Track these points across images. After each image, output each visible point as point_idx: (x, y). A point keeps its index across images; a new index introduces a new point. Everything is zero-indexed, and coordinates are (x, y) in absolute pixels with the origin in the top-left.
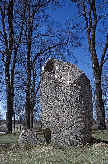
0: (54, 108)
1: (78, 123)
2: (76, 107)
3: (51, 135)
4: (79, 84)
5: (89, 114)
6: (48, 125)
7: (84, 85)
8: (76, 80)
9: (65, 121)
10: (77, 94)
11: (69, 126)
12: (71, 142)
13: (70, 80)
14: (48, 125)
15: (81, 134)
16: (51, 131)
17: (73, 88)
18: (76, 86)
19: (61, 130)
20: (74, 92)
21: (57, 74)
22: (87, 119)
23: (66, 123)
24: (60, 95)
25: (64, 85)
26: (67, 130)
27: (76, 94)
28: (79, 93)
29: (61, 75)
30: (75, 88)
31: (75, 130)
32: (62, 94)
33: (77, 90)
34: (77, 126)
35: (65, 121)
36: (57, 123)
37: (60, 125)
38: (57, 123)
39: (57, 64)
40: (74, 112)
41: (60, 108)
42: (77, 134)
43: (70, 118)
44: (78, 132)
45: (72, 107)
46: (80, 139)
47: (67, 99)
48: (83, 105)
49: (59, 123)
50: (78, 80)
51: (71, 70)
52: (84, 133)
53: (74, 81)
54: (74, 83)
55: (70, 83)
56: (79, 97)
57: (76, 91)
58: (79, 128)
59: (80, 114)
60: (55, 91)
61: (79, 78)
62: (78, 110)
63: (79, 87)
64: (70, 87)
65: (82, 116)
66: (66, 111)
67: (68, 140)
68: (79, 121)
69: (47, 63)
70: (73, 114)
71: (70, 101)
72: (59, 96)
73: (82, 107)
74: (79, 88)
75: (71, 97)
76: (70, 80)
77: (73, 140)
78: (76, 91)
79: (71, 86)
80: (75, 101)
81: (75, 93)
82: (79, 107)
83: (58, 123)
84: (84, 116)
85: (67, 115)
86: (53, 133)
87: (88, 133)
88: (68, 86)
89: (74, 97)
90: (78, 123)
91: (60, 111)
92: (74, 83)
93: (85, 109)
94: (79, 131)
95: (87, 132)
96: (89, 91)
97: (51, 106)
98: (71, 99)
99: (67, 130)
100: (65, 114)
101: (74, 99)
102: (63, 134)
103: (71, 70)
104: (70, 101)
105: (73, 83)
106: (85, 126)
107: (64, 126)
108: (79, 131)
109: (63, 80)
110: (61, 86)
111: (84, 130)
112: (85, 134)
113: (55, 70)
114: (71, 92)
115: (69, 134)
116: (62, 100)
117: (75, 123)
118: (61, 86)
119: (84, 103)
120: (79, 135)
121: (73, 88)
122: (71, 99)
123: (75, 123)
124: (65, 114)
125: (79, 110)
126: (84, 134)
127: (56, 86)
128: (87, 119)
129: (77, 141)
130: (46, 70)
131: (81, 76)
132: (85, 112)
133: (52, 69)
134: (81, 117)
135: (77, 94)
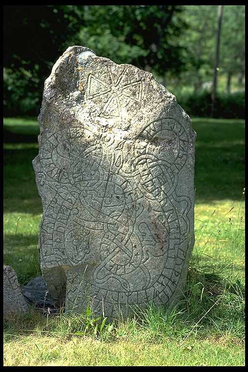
1: (145, 257)
3: (68, 286)
4: (153, 141)
5: (179, 227)
6: (58, 260)
7: (170, 142)
8: (144, 129)
9: (108, 250)
10: (146, 173)
13: (127, 129)
17: (134, 154)
18: (145, 147)
20: (137, 164)
21: (88, 103)
25: (110, 143)
27: (145, 170)
28: (152, 167)
29: (102, 108)
30: (141, 154)
33: (146, 159)
35: (108, 250)
43: (122, 241)
50: (150, 129)
51: (134, 94)
54: (140, 137)
55: (126, 139)
56: (151, 180)
57: (143, 164)
61: (157, 121)
64: (125, 151)
69: (61, 71)
74: (154, 153)
76: (127, 129)
78: (143, 164)
79: (129, 148)
87: (173, 283)
88: (119, 146)
89: (137, 181)
90: (145, 257)
92: (140, 137)
95: (170, 279)
96: (185, 157)
97: (67, 204)
99: (112, 275)
102: (100, 286)
105: (136, 139)
109: (106, 126)
111: (162, 275)
113: (84, 90)
117: (137, 255)
121: (137, 155)
123: (137, 255)
128: (172, 243)
130: (56, 95)
131: (160, 115)
132: (166, 225)
135: (146, 173)
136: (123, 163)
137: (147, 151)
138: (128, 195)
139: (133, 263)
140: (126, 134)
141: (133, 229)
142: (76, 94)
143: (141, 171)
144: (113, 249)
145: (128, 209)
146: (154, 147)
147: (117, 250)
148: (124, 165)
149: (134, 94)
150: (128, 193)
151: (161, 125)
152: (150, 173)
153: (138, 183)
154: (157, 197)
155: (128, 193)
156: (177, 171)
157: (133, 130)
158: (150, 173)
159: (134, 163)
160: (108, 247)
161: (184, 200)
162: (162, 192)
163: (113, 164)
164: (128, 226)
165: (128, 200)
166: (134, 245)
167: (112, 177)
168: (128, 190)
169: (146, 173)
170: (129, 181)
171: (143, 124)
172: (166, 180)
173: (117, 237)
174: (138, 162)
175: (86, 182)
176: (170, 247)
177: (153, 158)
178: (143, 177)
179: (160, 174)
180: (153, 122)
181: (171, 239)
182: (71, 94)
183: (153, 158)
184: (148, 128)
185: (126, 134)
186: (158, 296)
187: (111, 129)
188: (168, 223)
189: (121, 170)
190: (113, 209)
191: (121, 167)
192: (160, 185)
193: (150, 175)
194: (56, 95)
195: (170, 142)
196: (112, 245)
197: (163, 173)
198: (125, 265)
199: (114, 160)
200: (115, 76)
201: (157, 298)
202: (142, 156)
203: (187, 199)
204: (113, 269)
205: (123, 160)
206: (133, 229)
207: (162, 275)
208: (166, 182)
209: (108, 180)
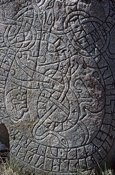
0: (13, 73)
1: (82, 114)
2: (75, 67)
3: (11, 142)
9: (45, 108)
10: (78, 29)
11: (56, 120)
12: (60, 162)
15: (91, 142)
16: (9, 132)
19: (34, 131)
20: (69, 21)
22: (108, 99)
23: (48, 113)
24: (29, 35)
25: (40, 3)
27: (77, 27)
28: (84, 23)
30: (72, 11)
31: (72, 132)
32: (34, 32)
33: (78, 15)
34: (79, 121)
36: (24, 112)
37: (32, 118)
38: (24, 112)
40: (69, 82)
41: (30, 72)
42: (79, 143)
43: (58, 99)
44: (81, 139)
45: (63, 67)
46: (87, 156)
47: (50, 44)
49: (29, 112)
52: (100, 140)
56: (84, 36)
57: (74, 20)
58: (83, 127)
59: (89, 86)
60: (15, 24)
62: (82, 76)
63: (85, 7)
64: (56, 9)
65: (93, 91)
66: (46, 79)
67: (53, 159)
68: (85, 107)
71: (57, 51)
72: (26, 38)
74: (86, 9)
75: (60, 38)
77: (66, 159)
78: (74, 20)
80: (72, 50)
81: (73, 25)
82: (84, 67)
83: (25, 114)
84: (100, 92)
85: (50, 90)
86: (14, 138)
87: (111, 137)
89: (70, 38)
90: (82, 114)
93: (102, 70)
94: (83, 136)
95: (108, 135)
98: (59, 45)
99: (51, 132)
100: (44, 88)
101: (68, 43)
102: (40, 141)
104: (57, 51)
106: (103, 120)
107: (41, 120)
108: (83, 136)
110: (32, 9)
111: (100, 130)
112: (102, 142)
114: (59, 22)
115: (55, 142)
116: (35, 47)
117: (74, 112)
118: (32, 9)
119: (101, 54)
120: (84, 145)
121: (67, 11)
122: (59, 45)
123: (74, 112)
124: (44, 88)
125: (85, 74)
126: (99, 141)
127: (17, 9)
129: (78, 162)
132: (102, 81)
134: (90, 95)
135: (78, 29)
136: (54, 21)
137: (78, 8)
138: (62, 53)
139: (70, 120)
141: (69, 87)
143: (73, 28)
144: (50, 107)
145: (63, 67)
146: (84, 4)
147: (54, 108)
148: (56, 22)
150: (61, 51)
152: (83, 30)
153: (71, 40)
154: (91, 54)
155: (61, 51)
156: (109, 29)
158: (83, 30)
159: (66, 20)
160: (45, 105)
163: (45, 23)
165: (61, 57)
166: (70, 102)
167: (44, 36)
168: (62, 48)
169: (79, 30)
170: (62, 38)
172: (99, 38)
173: (52, 95)
174: (70, 19)
176: (107, 103)
178: (76, 34)
179: (93, 31)
181: (107, 95)
183: (85, 14)
186: (97, 151)
188: (104, 80)
189: (53, 28)
191: (53, 25)
192: (93, 42)
193: (83, 31)
196: (48, 103)
197: (95, 29)
198: (62, 122)
199: (46, 18)
204: (51, 127)
205: (54, 18)
206: (69, 87)
207: (100, 130)
208: (99, 39)
209: (40, 39)
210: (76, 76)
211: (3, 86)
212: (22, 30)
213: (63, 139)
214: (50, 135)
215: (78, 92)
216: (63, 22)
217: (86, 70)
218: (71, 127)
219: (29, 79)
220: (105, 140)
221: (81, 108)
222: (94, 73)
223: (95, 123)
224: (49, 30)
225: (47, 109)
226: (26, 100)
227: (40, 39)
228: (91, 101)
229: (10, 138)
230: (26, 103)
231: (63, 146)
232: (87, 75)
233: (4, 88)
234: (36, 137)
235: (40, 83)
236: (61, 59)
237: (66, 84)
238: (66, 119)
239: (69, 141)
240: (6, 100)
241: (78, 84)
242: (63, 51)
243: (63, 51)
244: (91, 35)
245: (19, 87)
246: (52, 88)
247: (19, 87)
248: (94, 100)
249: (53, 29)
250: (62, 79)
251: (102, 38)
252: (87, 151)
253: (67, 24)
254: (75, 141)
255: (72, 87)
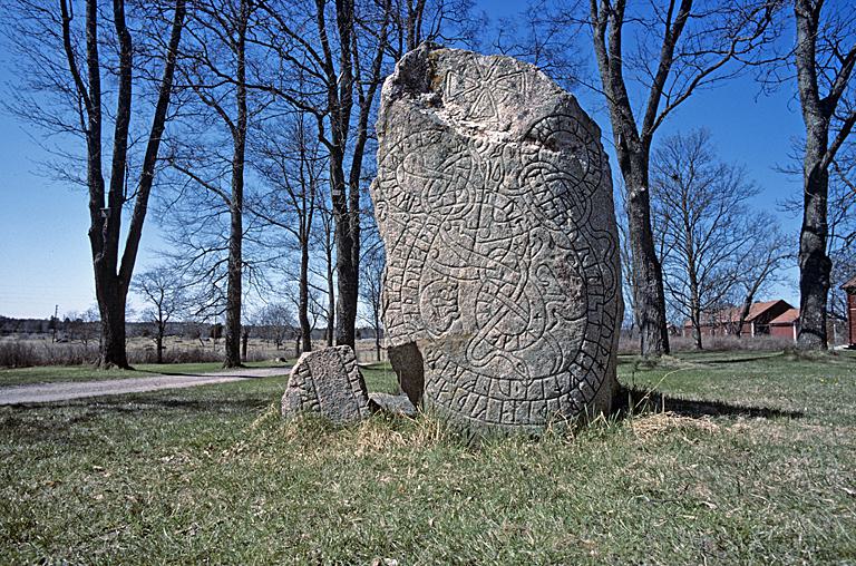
1: (551, 320)
2: (537, 246)
3: (426, 373)
4: (551, 145)
5: (600, 277)
6: (409, 331)
7: (574, 149)
8: (533, 126)
9: (489, 311)
10: (542, 188)
11: (508, 331)
12: (515, 406)
13: (508, 128)
14: (409, 331)
15: (566, 369)
16: (424, 356)
18: (537, 151)
19: (469, 351)
20: (526, 176)
22: (593, 300)
23: (493, 320)
26: (499, 352)
27: (539, 185)
28: (550, 180)
29: (469, 110)
30: (532, 161)
33: (541, 168)
36: (452, 318)
37: (466, 328)
38: (452, 318)
39: (450, 68)
42: (546, 371)
43: (510, 296)
44: (551, 363)
45: (517, 245)
47: (496, 210)
48: (571, 235)
49: (461, 319)
53: (524, 132)
55: (506, 140)
56: (551, 200)
57: (535, 175)
58: (553, 343)
60: (441, 177)
61: (552, 116)
62: (548, 260)
63: (551, 156)
64: (506, 159)
66: (491, 264)
67: (503, 401)
68: (554, 310)
69: (406, 64)
70: (524, 277)
71: (508, 220)
72: (458, 200)
73: (568, 245)
74: (552, 160)
75: (513, 201)
76: (508, 128)
77: (525, 399)
78: (535, 175)
79: (513, 153)
80: (532, 219)
81: (533, 182)
83: (454, 322)
86: (433, 367)
87: (600, 366)
88: (497, 151)
89: (528, 201)
90: (551, 320)
91: (465, 266)
92: (528, 137)
94: (553, 357)
95: (594, 360)
97: (421, 243)
98: (512, 211)
99: (499, 352)
100: (488, 279)
101: (526, 209)
102: (480, 370)
103: (514, 86)
105: (521, 140)
107: (482, 332)
108: (553, 357)
109: (476, 128)
110: (467, 156)
111: (581, 351)
112: (585, 372)
113: (441, 91)
114: (511, 177)
115: (507, 369)
116: (472, 216)
117: (536, 317)
118: (467, 156)
119: (578, 229)
124: (488, 279)
125: (553, 257)
127: (444, 156)
131: (556, 108)
133: (429, 89)
135: (542, 188)
137: (540, 157)
140: (507, 134)
142: (429, 96)
146: (550, 152)
147: (503, 310)
148: (506, 177)
149: (514, 86)
151: (558, 123)
157: (514, 129)
159: (522, 174)
161: (605, 237)
162: (569, 220)
164: (519, 271)
171: (527, 120)
175: (449, 207)
177: (551, 167)
180: (546, 118)
182: (423, 94)
183: (551, 167)
184: (539, 124)
185: (507, 134)
187: (482, 132)
188: (584, 268)
190: (493, 244)
194: (400, 94)
195: (574, 149)
198: (518, 335)
200: (484, 67)
201: (576, 390)
202: (533, 164)
203: (608, 235)
204: (498, 342)
209: (481, 202)
210: (539, 260)
211: (417, 276)
212: (451, 187)
213: (519, 364)
214: (497, 358)
215: (544, 286)
216: (517, 178)
217: (556, 251)
218: (533, 342)
219: (462, 265)
220: (591, 368)
221: (549, 312)
222: (567, 257)
223: (573, 336)
224: (495, 189)
225: (493, 313)
226: (456, 298)
227: (481, 202)
228: (564, 301)
229: (425, 366)
230: (456, 303)
231: (521, 377)
232: (557, 259)
233: (418, 280)
234: (473, 361)
235: (481, 270)
236: (515, 233)
237: (522, 272)
238: (525, 330)
239: (529, 366)
240: (422, 300)
241: (542, 272)
242: (518, 221)
243: (518, 221)
244: (562, 198)
245: (445, 278)
246: (501, 278)
247: (445, 278)
248: (568, 300)
249: (501, 186)
250: (517, 265)
251: (578, 203)
252: (560, 385)
253: (523, 180)
254: (539, 367)
255: (534, 278)
